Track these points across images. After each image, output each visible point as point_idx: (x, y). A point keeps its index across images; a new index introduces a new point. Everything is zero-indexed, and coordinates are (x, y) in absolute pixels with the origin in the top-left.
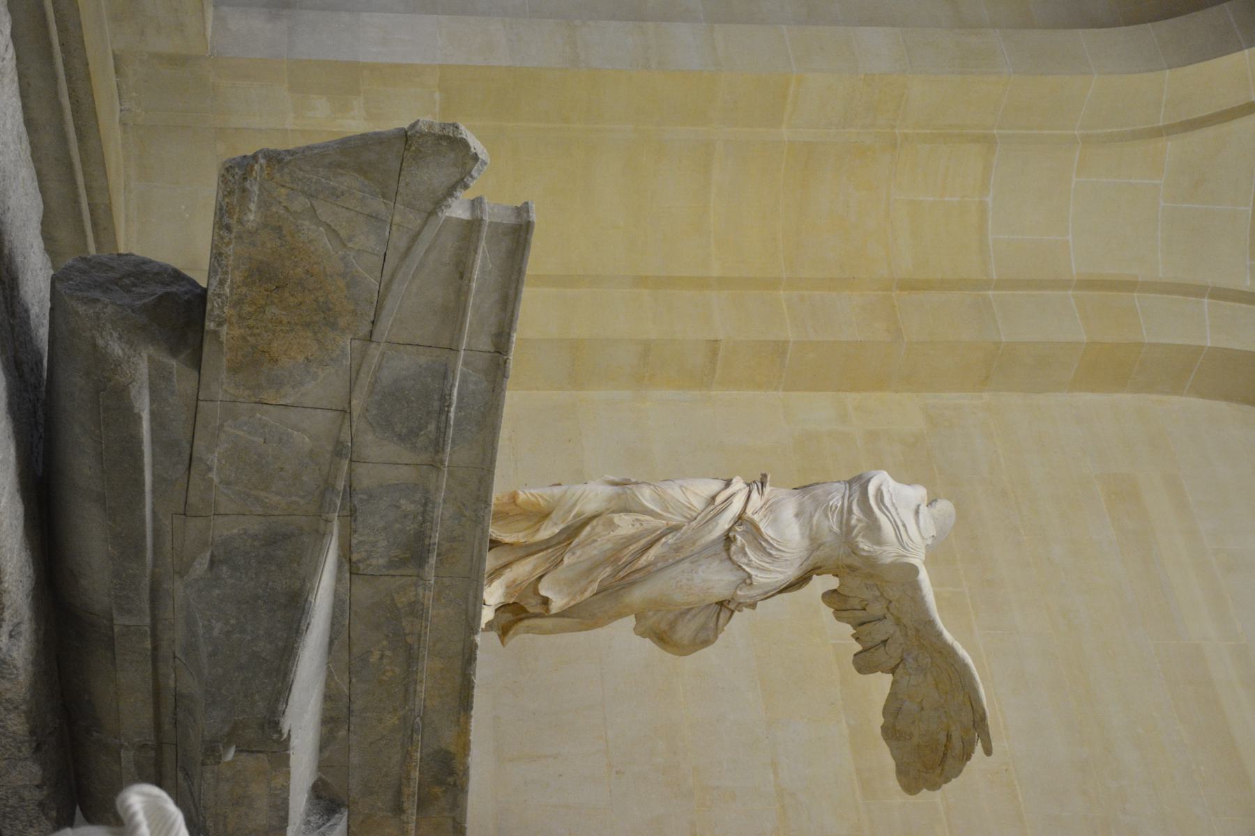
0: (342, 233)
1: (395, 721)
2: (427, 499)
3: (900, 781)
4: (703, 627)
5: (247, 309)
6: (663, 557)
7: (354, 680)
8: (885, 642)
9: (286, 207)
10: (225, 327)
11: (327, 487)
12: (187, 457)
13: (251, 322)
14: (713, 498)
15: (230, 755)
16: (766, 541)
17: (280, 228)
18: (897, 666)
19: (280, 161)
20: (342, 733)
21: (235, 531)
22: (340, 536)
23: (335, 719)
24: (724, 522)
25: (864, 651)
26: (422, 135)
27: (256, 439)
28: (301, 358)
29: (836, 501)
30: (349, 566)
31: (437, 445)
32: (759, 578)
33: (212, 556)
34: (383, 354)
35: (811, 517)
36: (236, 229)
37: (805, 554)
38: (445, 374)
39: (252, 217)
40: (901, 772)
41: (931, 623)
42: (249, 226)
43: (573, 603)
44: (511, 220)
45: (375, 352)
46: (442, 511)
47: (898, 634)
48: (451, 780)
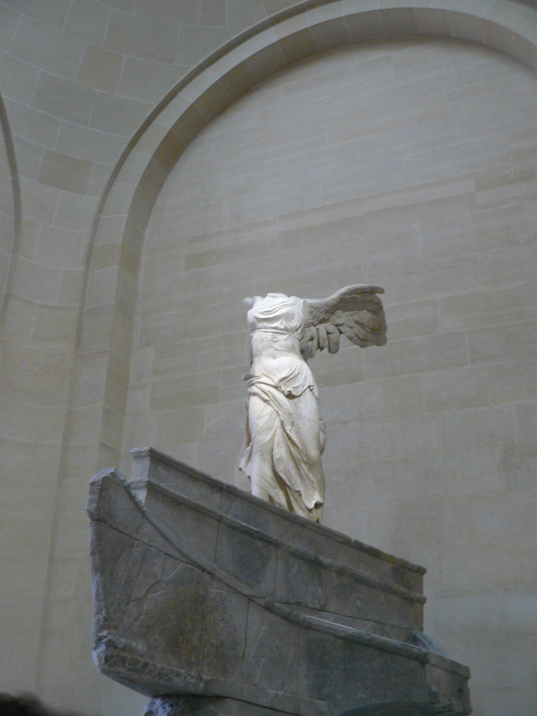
1: (383, 596)
6: (297, 433)
7: (368, 617)
8: (328, 333)
9: (136, 620)
10: (203, 676)
12: (270, 710)
14: (265, 401)
16: (291, 375)
18: (339, 329)
19: (106, 619)
21: (305, 682)
24: (280, 397)
26: (97, 508)
29: (269, 336)
31: (268, 541)
35: (277, 350)
38: (233, 527)
39: (140, 646)
44: (147, 462)
45: (219, 573)
47: (327, 325)
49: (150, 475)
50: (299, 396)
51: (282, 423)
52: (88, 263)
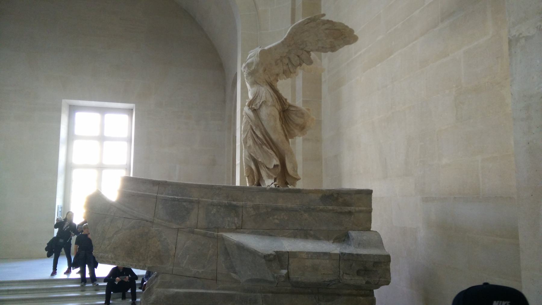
2: (211, 205)
3: (352, 43)
8: (298, 56)
11: (205, 235)
15: (284, 272)
17: (114, 248)
18: (306, 51)
20: (312, 232)
23: (305, 234)
25: (304, 62)
30: (238, 229)
31: (191, 202)
32: (263, 99)
33: (233, 273)
40: (349, 43)
41: (282, 42)
42: (113, 256)
43: (275, 157)
46: (215, 201)
48: (335, 196)
50: (259, 109)
51: (251, 126)
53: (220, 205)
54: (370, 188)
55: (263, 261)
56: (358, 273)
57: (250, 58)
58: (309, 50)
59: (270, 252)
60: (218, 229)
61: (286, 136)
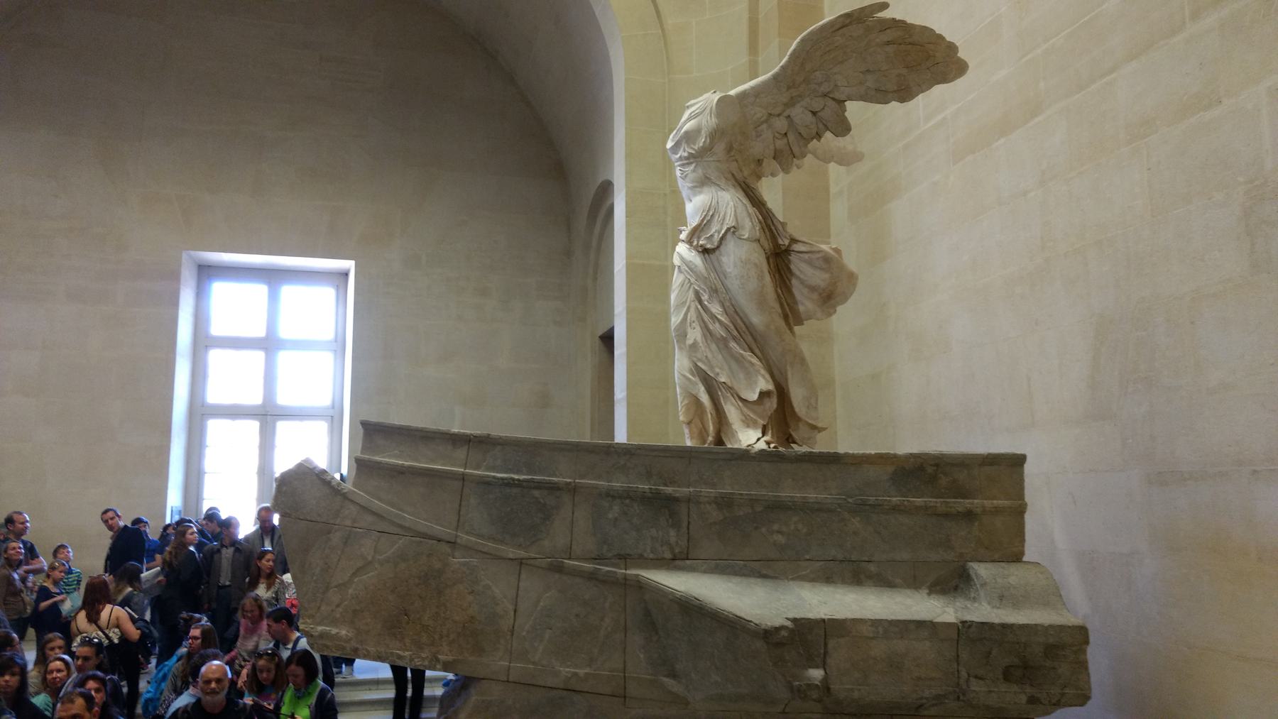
0: (360, 564)
2: (608, 495)
4: (810, 263)
5: (424, 639)
8: (814, 113)
9: (338, 606)
11: (592, 577)
13: (437, 637)
15: (816, 674)
17: (355, 611)
18: (833, 99)
20: (872, 568)
22: (647, 567)
23: (856, 573)
25: (827, 129)
27: (547, 636)
28: (470, 598)
30: (678, 560)
31: (553, 488)
32: (729, 222)
34: (467, 533)
36: (354, 644)
37: (713, 189)
38: (486, 483)
40: (945, 79)
43: (763, 372)
45: (464, 538)
48: (930, 470)
49: (364, 449)
50: (718, 247)
52: (753, 47)
53: (629, 497)
54: (1019, 451)
55: (759, 644)
56: (1007, 676)
57: (689, 119)
58: (842, 97)
59: (778, 622)
60: (625, 559)
61: (786, 317)
